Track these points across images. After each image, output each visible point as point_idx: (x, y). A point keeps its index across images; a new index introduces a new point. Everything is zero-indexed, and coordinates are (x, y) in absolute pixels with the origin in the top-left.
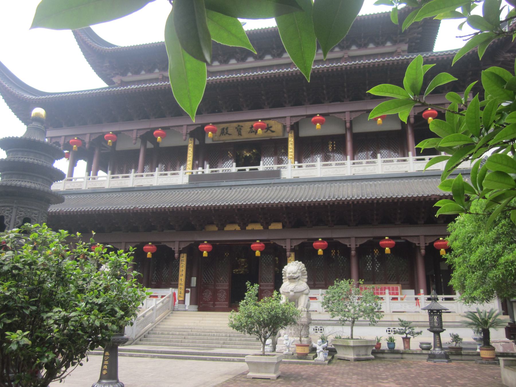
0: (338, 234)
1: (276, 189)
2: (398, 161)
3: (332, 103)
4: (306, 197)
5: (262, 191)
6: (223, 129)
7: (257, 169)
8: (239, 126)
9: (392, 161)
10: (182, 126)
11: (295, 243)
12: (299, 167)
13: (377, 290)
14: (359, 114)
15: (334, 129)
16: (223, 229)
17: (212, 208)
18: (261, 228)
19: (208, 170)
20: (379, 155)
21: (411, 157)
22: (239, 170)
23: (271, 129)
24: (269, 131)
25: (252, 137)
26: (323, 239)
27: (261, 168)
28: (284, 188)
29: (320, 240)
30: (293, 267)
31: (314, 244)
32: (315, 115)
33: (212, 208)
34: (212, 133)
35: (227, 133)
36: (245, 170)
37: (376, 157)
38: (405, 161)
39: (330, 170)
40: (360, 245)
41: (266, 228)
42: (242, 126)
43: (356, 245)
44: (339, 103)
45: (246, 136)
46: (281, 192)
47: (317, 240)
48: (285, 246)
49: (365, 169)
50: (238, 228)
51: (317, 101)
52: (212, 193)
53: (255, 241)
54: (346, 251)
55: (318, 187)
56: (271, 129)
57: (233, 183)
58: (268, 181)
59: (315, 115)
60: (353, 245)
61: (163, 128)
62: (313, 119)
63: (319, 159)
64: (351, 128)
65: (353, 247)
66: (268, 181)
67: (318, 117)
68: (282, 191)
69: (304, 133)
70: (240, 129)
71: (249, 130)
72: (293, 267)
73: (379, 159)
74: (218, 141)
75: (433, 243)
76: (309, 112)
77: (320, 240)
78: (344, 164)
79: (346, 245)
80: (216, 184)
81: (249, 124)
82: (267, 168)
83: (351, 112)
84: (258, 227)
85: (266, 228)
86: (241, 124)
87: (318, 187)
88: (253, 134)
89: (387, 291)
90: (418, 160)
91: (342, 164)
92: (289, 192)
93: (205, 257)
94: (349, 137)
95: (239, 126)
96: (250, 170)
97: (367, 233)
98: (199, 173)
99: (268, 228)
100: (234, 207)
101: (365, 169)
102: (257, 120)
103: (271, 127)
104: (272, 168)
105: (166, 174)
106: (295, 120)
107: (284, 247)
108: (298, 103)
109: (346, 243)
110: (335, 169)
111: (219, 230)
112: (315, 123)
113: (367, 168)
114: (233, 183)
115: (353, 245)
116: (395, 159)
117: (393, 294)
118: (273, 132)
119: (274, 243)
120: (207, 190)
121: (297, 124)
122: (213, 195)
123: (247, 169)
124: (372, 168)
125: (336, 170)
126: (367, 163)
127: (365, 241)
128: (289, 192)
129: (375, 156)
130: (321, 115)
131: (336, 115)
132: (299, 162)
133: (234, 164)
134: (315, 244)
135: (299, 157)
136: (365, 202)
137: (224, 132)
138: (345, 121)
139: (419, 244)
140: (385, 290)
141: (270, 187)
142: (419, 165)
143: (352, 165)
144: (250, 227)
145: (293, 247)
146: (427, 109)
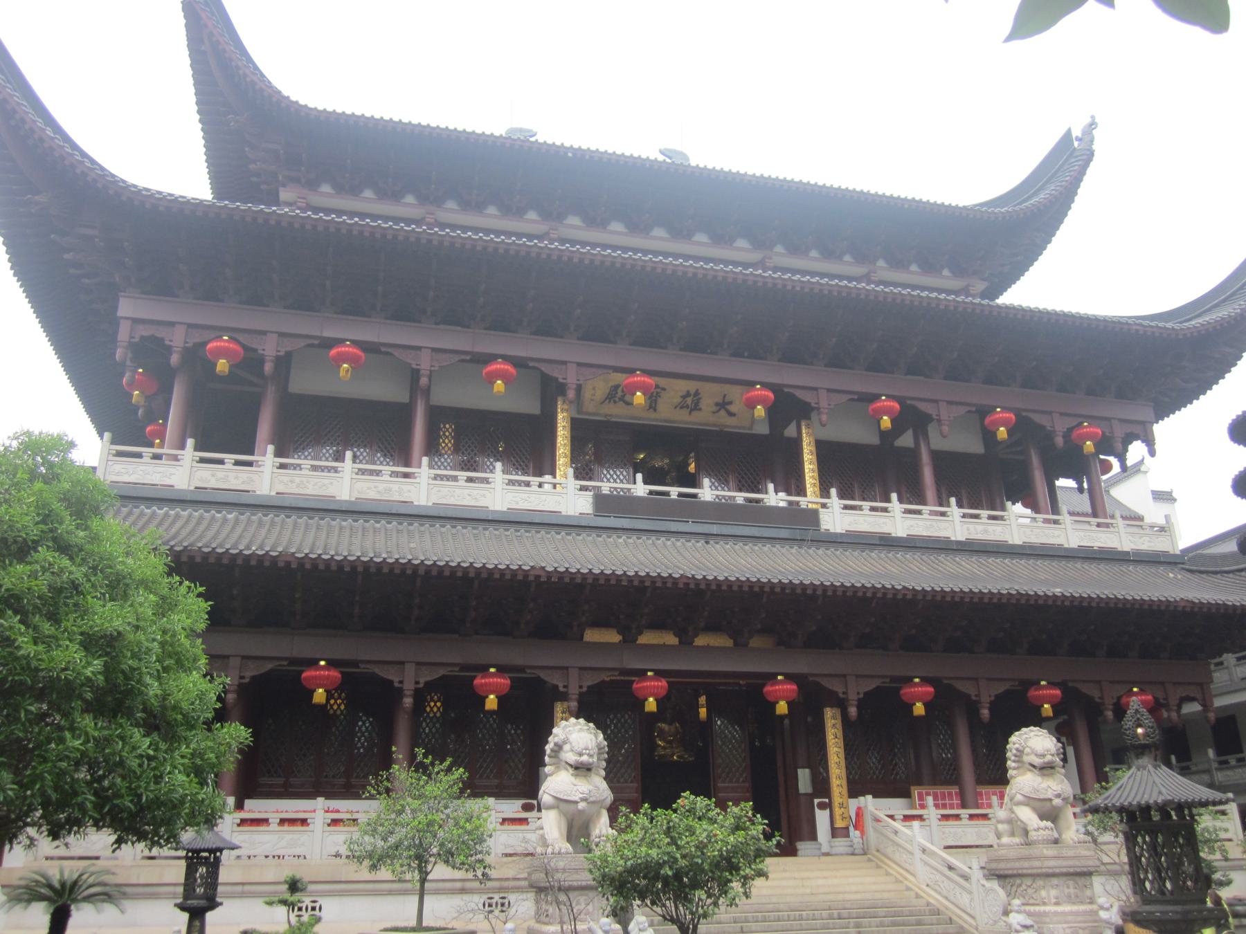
0: (370, 652)
1: (249, 522)
2: (393, 474)
3: (442, 326)
5: (205, 523)
6: (616, 387)
7: (695, 496)
8: (657, 387)
9: (378, 473)
10: (264, 333)
11: (590, 680)
13: (943, 798)
14: (457, 358)
15: (382, 389)
16: (746, 645)
19: (640, 489)
20: (349, 454)
21: (267, 458)
22: (651, 493)
25: (683, 419)
26: (331, 663)
27: (707, 492)
29: (322, 663)
34: (644, 394)
35: (622, 399)
37: (888, 500)
38: (406, 475)
39: (920, 523)
40: (253, 678)
41: (629, 639)
42: (664, 389)
44: (459, 328)
45: (706, 417)
47: (313, 663)
48: (401, 682)
50: (671, 639)
51: (354, 309)
52: (209, 525)
53: (642, 673)
55: (341, 528)
56: (732, 408)
57: (715, 529)
58: (625, 523)
60: (409, 680)
61: (370, 348)
62: (334, 351)
64: (427, 392)
65: (409, 686)
66: (625, 523)
69: (305, 382)
70: (658, 395)
71: (677, 400)
74: (594, 414)
76: (328, 333)
77: (322, 663)
78: (336, 470)
79: (392, 682)
80: (674, 527)
81: (684, 386)
83: (190, 326)
84: (613, 637)
85: (629, 639)
87: (341, 528)
88: (685, 412)
89: (930, 800)
90: (202, 460)
91: (329, 469)
95: (657, 387)
96: (680, 495)
101: (986, 531)
102: (631, 371)
103: (730, 403)
105: (977, 517)
106: (288, 345)
107: (396, 685)
108: (304, 303)
109: (392, 675)
110: (929, 523)
111: (624, 641)
112: (491, 379)
113: (990, 528)
115: (409, 680)
117: (944, 806)
119: (818, 684)
121: (289, 355)
122: (202, 528)
123: (674, 491)
126: (314, 468)
129: (339, 457)
130: (354, 342)
131: (397, 353)
133: (639, 476)
134: (906, 691)
135: (288, 443)
136: (778, 590)
137: (692, 402)
138: (418, 371)
140: (988, 798)
141: (322, 519)
142: (912, 522)
143: (195, 464)
144: (700, 641)
145: (421, 686)
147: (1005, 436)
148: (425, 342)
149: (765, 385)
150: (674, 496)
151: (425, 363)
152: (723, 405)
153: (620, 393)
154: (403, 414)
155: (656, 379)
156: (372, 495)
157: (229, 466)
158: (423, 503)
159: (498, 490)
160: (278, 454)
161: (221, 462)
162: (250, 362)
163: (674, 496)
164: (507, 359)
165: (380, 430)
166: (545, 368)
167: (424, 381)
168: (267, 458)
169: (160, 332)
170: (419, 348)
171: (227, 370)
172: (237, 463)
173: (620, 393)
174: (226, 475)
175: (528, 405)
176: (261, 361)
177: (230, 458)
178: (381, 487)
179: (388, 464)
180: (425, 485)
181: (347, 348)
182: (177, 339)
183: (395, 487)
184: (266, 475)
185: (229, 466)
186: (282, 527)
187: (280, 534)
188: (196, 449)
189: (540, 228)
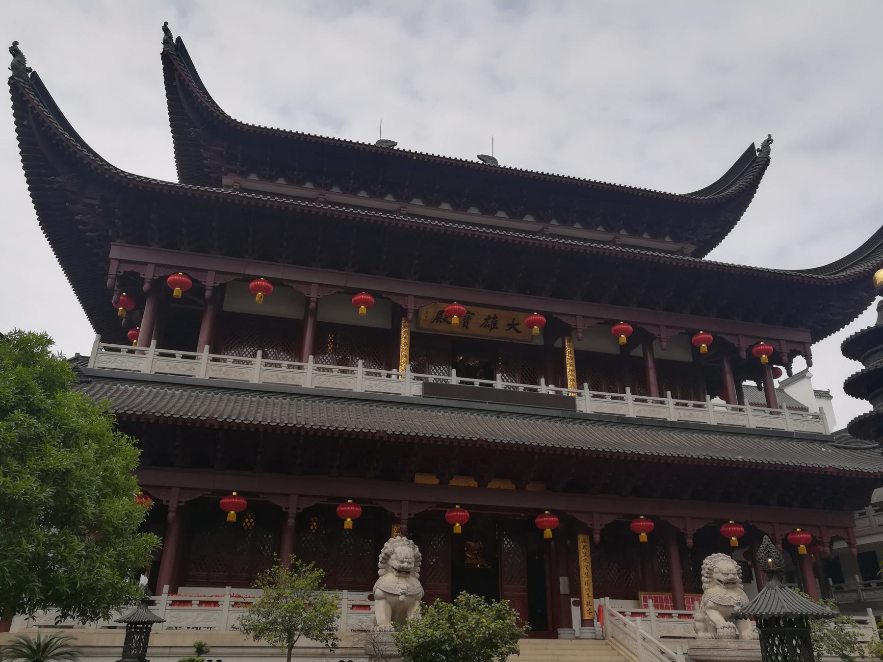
4: (186, 414)
5: (160, 397)
7: (491, 385)
8: (468, 312)
9: (280, 366)
12: (389, 376)
17: (416, 441)
18: (512, 487)
19: (454, 379)
20: (259, 353)
21: (204, 354)
22: (461, 382)
23: (516, 327)
24: (512, 330)
25: (486, 333)
27: (499, 383)
28: (244, 400)
30: (400, 549)
31: (339, 509)
32: (258, 278)
33: (416, 441)
35: (445, 320)
36: (472, 383)
38: (299, 368)
41: (444, 482)
43: (180, 502)
45: (500, 333)
46: (191, 402)
49: (691, 415)
50: (474, 484)
51: (267, 257)
52: (163, 398)
54: (281, 515)
55: (251, 402)
56: (519, 328)
57: (503, 408)
58: (444, 402)
59: (258, 278)
62: (252, 284)
63: (360, 362)
64: (315, 312)
66: (444, 402)
67: (261, 283)
68: (255, 406)
69: (233, 304)
71: (482, 321)
72: (400, 549)
73: (360, 368)
74: (426, 329)
75: (787, 535)
76: (250, 272)
77: (234, 494)
78: (248, 363)
82: (508, 386)
83: (157, 265)
85: (444, 482)
86: (472, 309)
87: (251, 402)
88: (487, 329)
90: (161, 355)
92: (223, 405)
93: (644, 543)
94: (650, 363)
95: (468, 312)
96: (481, 384)
97: (202, 482)
98: (551, 393)
99: (412, 480)
100: (337, 435)
102: (451, 302)
103: (518, 324)
104: (517, 387)
106: (222, 280)
114: (503, 408)
116: (285, 363)
118: (518, 332)
120: (456, 415)
121: (223, 286)
122: (157, 399)
123: (477, 382)
124: (701, 414)
125: (691, 415)
127: (198, 495)
128: (223, 405)
130: (266, 279)
132: (557, 386)
133: (454, 371)
135: (220, 346)
139: (168, 501)
141: (239, 396)
143: (156, 357)
146: (758, 343)
147: (625, 341)
148: (315, 280)
149: (540, 313)
150: (477, 385)
151: (313, 294)
152: (512, 325)
153: (444, 317)
154: (298, 327)
155: (468, 307)
156: (274, 380)
157: (178, 359)
158: (308, 386)
159: (360, 379)
160: (211, 351)
161: (173, 356)
162: (195, 290)
163: (477, 385)
164: (368, 292)
165: (280, 337)
166: (394, 298)
167: (312, 305)
168: (204, 354)
169: (137, 269)
170: (310, 283)
171: (180, 295)
172: (184, 357)
173: (444, 317)
174: (176, 365)
175: (382, 322)
176: (203, 289)
177: (179, 353)
178: (280, 375)
179: (288, 360)
180: (310, 375)
181: (261, 283)
182: (148, 274)
183: (290, 375)
184: (203, 366)
185: (178, 359)
186: (212, 400)
187: (210, 404)
188: (157, 347)
189: (394, 206)
